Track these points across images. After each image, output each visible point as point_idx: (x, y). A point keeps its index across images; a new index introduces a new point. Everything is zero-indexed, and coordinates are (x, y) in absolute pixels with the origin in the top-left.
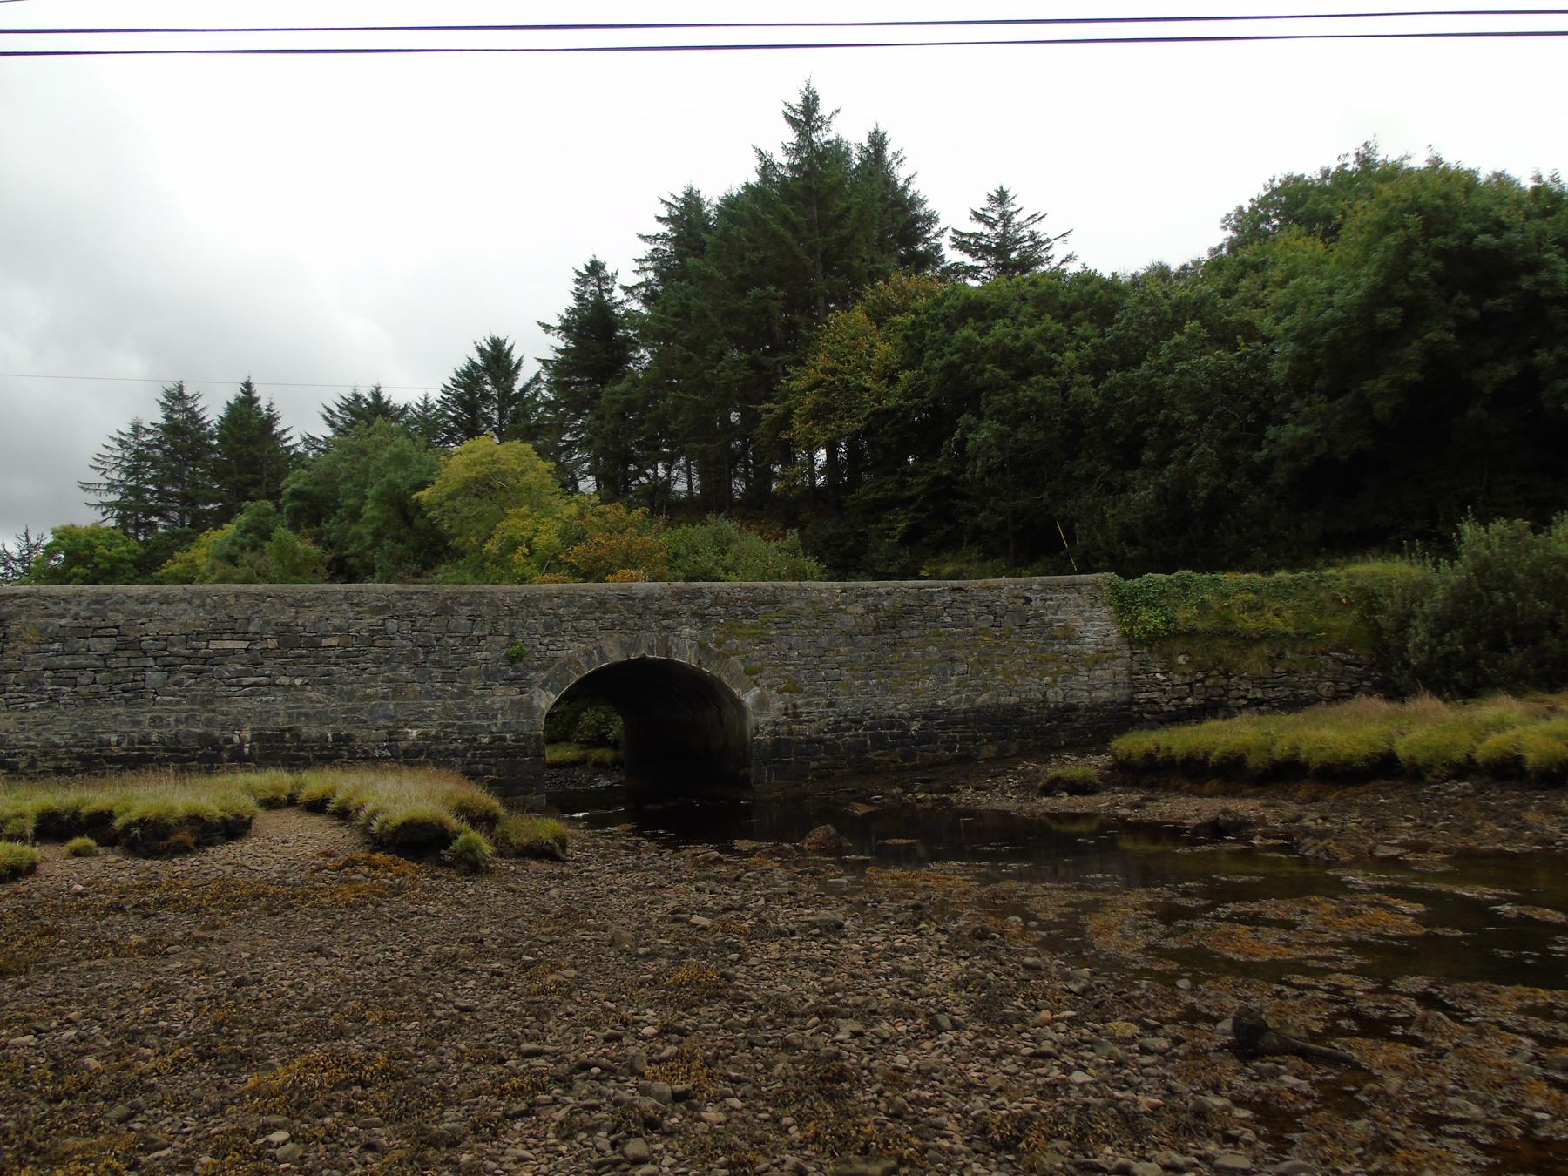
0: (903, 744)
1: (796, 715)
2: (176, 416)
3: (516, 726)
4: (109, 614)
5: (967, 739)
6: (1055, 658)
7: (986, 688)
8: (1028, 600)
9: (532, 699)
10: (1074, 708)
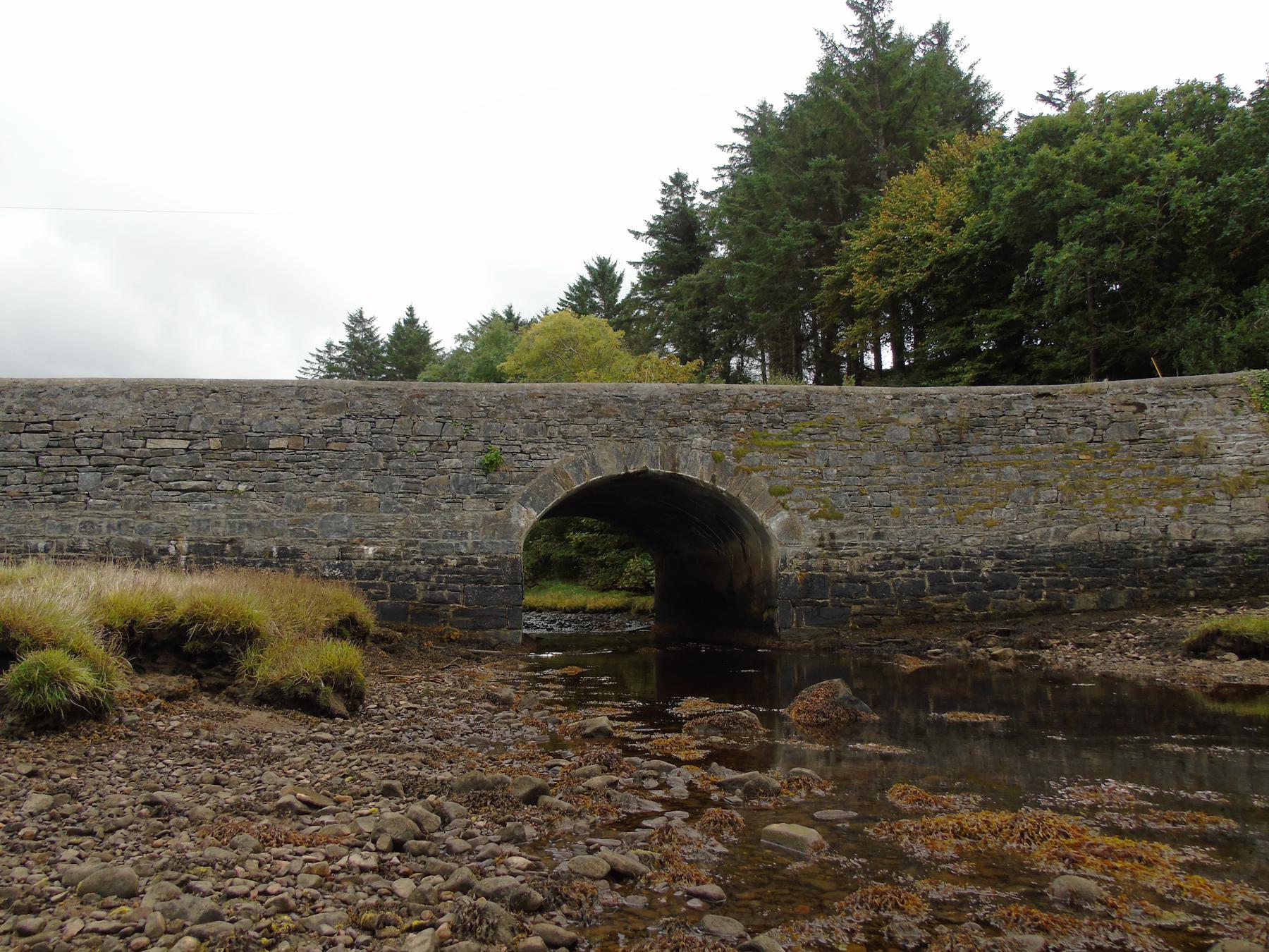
0: (972, 588)
1: (834, 547)
2: (357, 335)
3: (490, 548)
4: (43, 408)
5: (1056, 584)
6: (1180, 482)
7: (1083, 520)
8: (1141, 408)
9: (510, 516)
10: (1208, 548)
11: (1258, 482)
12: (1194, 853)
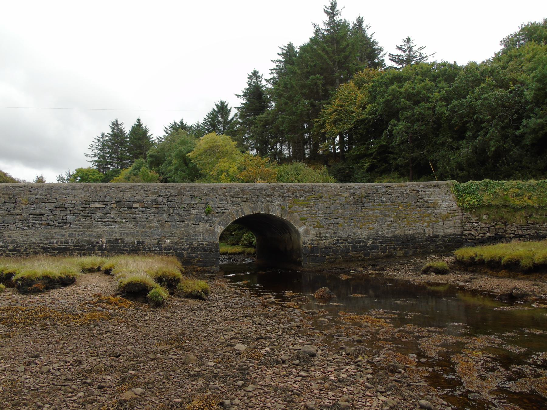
0: (365, 250)
1: (321, 237)
2: (115, 131)
3: (208, 239)
4: (53, 194)
5: (391, 248)
6: (429, 216)
7: (400, 227)
8: (418, 192)
9: (215, 229)
10: (437, 237)
11: (452, 216)
12: (387, 320)
